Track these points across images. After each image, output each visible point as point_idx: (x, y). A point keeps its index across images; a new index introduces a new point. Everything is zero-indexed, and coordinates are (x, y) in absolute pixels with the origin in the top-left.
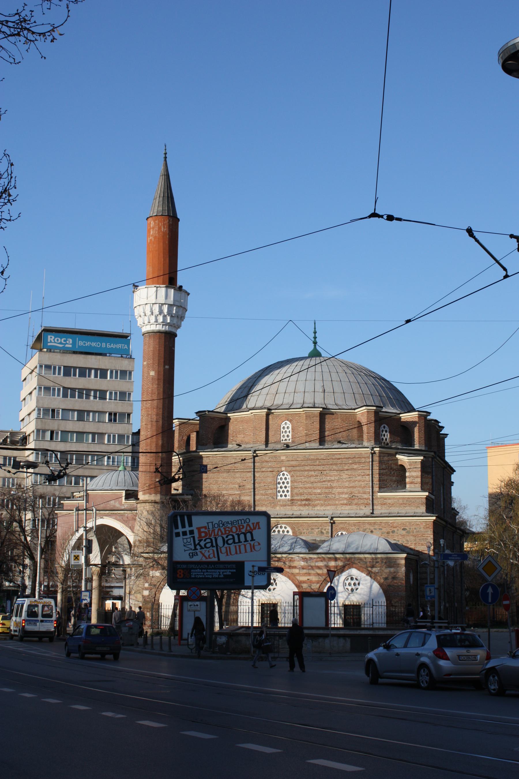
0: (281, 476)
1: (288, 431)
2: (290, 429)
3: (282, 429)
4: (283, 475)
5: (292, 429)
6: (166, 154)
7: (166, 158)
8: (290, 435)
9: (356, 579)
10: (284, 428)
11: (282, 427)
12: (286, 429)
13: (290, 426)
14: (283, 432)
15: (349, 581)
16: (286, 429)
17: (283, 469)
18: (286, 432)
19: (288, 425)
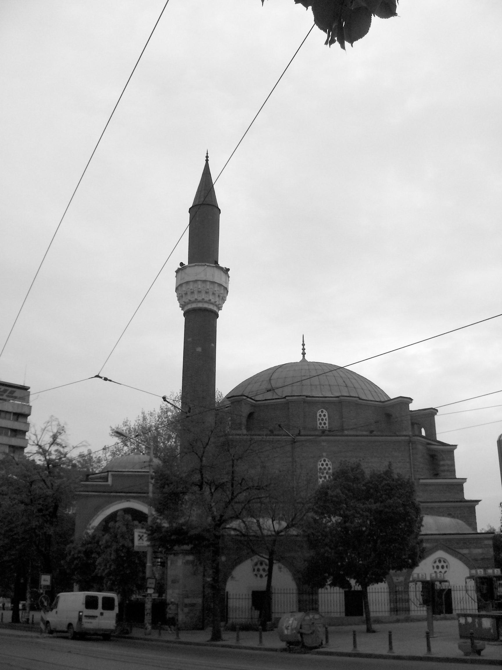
0: (323, 462)
1: (324, 418)
2: (327, 417)
3: (318, 417)
4: (325, 461)
5: (329, 417)
6: (207, 157)
7: (207, 161)
8: (327, 422)
9: (444, 562)
10: (320, 415)
11: (318, 415)
12: (322, 417)
13: (327, 414)
14: (319, 419)
15: (438, 563)
16: (322, 417)
17: (324, 454)
18: (322, 420)
19: (324, 413)
